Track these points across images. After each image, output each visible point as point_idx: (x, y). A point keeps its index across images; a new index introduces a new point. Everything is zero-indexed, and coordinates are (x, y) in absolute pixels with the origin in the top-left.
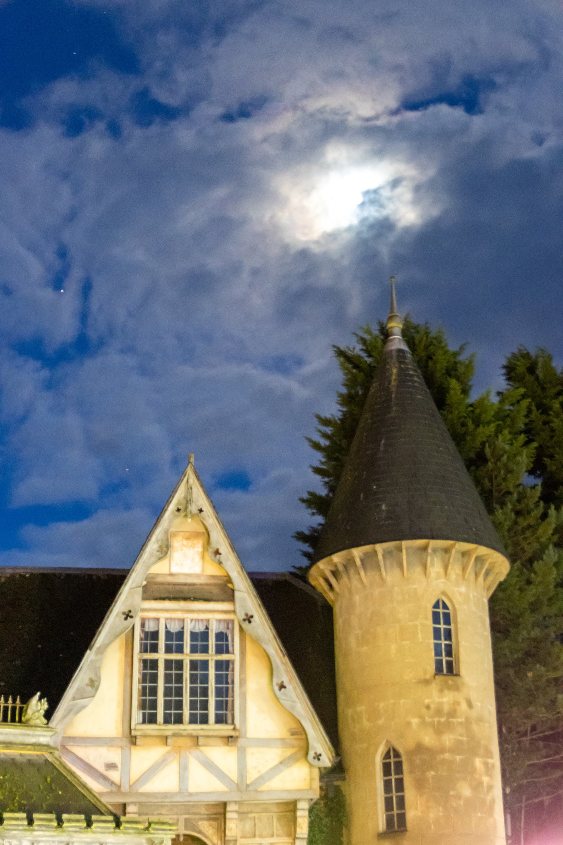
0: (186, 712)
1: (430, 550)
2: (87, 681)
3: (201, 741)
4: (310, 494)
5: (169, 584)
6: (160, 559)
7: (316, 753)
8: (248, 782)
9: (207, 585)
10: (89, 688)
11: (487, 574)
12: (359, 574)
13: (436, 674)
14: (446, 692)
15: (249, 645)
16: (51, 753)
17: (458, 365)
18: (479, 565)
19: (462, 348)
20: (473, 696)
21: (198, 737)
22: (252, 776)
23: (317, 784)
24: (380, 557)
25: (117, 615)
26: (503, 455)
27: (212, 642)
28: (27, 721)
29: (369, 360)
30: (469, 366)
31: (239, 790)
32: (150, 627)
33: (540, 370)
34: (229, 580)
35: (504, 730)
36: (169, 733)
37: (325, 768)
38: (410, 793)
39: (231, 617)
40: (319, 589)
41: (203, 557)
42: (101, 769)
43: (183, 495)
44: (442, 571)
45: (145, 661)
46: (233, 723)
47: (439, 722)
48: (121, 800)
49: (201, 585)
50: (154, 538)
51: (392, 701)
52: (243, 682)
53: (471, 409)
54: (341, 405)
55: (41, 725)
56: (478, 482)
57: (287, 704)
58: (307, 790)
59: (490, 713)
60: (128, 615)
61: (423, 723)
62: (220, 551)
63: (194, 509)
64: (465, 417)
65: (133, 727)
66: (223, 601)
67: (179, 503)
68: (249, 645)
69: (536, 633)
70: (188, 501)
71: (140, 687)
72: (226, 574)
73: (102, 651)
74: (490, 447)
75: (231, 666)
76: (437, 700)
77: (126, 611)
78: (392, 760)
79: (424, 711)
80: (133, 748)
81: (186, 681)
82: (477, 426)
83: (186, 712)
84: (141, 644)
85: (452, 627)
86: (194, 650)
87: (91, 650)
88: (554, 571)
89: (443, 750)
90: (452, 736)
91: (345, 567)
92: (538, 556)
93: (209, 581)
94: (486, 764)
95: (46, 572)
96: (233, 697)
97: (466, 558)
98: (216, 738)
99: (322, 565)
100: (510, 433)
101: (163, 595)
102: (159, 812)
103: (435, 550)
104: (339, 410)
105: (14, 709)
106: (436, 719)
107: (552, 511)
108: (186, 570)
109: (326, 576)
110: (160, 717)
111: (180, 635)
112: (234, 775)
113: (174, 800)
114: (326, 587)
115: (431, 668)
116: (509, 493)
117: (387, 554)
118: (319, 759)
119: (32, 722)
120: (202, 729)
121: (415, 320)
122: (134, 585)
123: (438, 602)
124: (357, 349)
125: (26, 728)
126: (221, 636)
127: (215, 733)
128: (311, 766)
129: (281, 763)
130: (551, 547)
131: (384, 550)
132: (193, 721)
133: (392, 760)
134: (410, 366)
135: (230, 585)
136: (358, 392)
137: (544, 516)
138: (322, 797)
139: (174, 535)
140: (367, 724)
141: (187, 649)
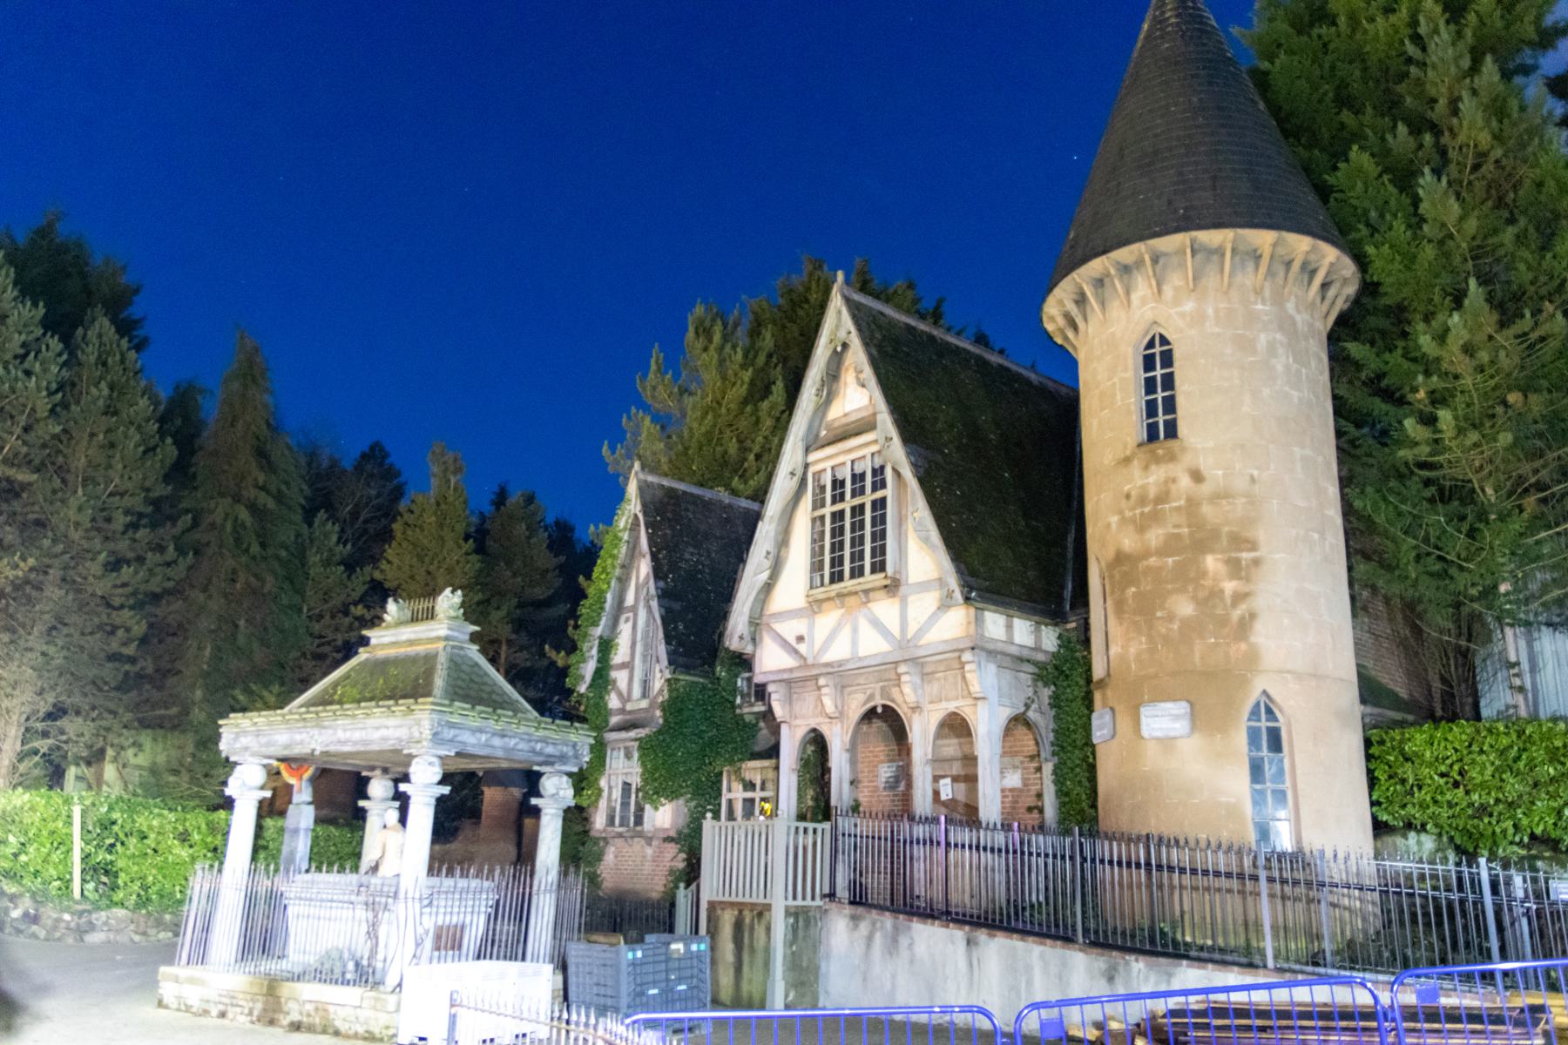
14: (1153, 467)
31: (901, 648)
42: (793, 641)
76: (1140, 483)
90: (1160, 532)
112: (896, 633)
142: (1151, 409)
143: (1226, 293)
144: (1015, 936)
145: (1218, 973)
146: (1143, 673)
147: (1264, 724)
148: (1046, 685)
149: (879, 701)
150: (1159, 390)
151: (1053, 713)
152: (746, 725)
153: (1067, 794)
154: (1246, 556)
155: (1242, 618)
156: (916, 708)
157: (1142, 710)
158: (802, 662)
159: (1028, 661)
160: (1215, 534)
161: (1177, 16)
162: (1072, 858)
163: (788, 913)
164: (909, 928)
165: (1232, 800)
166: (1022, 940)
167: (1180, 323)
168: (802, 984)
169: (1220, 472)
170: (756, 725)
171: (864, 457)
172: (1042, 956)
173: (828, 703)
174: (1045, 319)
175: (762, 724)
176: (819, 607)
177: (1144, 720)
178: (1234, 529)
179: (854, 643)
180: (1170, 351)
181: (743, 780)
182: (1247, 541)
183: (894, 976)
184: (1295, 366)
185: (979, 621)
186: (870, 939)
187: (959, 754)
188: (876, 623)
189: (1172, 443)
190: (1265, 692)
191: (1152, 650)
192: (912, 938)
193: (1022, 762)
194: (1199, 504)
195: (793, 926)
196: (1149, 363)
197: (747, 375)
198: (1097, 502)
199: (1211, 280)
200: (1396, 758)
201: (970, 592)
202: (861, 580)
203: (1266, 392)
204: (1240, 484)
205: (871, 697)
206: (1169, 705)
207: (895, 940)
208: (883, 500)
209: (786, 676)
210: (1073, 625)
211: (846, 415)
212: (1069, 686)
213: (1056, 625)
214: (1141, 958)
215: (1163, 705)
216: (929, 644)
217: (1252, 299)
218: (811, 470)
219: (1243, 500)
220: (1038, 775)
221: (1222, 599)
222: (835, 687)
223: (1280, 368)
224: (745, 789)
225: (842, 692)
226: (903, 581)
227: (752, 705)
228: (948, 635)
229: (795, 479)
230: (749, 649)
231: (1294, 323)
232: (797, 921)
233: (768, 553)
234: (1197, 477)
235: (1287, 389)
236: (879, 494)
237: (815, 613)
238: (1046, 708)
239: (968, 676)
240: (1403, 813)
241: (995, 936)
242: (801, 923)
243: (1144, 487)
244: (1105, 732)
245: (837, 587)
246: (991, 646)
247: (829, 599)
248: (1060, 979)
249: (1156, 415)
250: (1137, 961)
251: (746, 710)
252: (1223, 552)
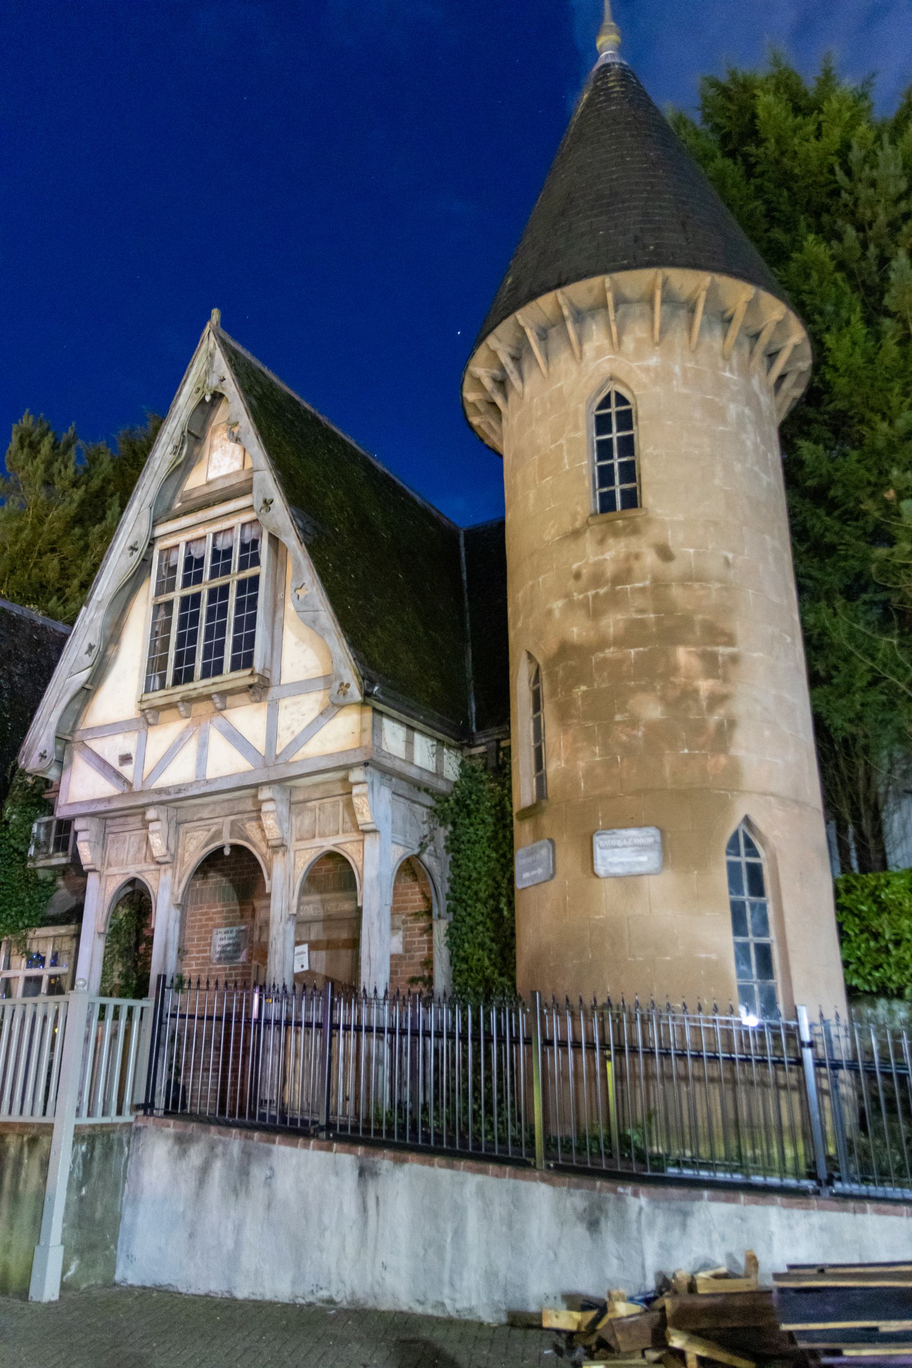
14: (611, 541)
76: (592, 559)
79: (571, 583)
112: (260, 745)
129: (321, 714)
142: (605, 475)
143: (694, 352)
144: (437, 1160)
145: (754, 1207)
146: (597, 792)
147: (744, 859)
148: (443, 822)
149: (227, 840)
150: (616, 455)
151: (449, 858)
152: (38, 883)
153: (465, 960)
154: (723, 650)
155: (720, 725)
156: (279, 847)
157: (596, 839)
158: (126, 789)
159: (426, 790)
160: (687, 622)
161: (621, 86)
162: (464, 1039)
163: (79, 1136)
164: (269, 1153)
165: (714, 957)
166: (451, 1167)
167: (644, 378)
168: (92, 1247)
169: (692, 551)
170: (52, 883)
171: (231, 529)
172: (480, 1191)
173: (158, 844)
174: (467, 382)
175: (60, 882)
176: (156, 717)
177: (598, 852)
178: (708, 617)
179: (201, 760)
180: (629, 412)
181: (28, 954)
182: (723, 633)
183: (239, 1229)
184: (762, 448)
185: (376, 729)
186: (204, 1170)
187: (321, 913)
188: (235, 738)
189: (632, 512)
190: (747, 820)
191: (609, 764)
192: (271, 1169)
193: (404, 922)
194: (667, 586)
195: (84, 1156)
196: (602, 424)
197: (78, 494)
198: (532, 587)
199: (678, 336)
200: (870, 908)
201: (372, 683)
202: (217, 679)
203: (738, 467)
204: (714, 566)
205: (218, 835)
206: (633, 832)
207: (244, 1172)
208: (255, 580)
209: (101, 807)
210: (481, 749)
211: (209, 483)
212: (472, 825)
213: (460, 748)
214: (642, 1190)
215: (624, 833)
216: (305, 760)
217: (721, 363)
218: (159, 546)
219: (718, 585)
220: (425, 937)
221: (696, 700)
222: (169, 823)
223: (749, 444)
224: (29, 966)
225: (177, 831)
226: (274, 681)
227: (49, 857)
229: (136, 554)
230: (52, 774)
231: (759, 403)
232: (91, 1149)
233: (91, 647)
234: (665, 554)
235: (756, 469)
236: (249, 573)
237: (149, 724)
238: (442, 852)
239: (356, 800)
240: (877, 974)
241: (404, 1161)
242: (98, 1152)
243: (600, 564)
244: (540, 871)
245: (183, 689)
246: (388, 763)
247: (171, 706)
248: (510, 1227)
249: (612, 483)
250: (636, 1194)
251: (40, 864)
252: (696, 644)
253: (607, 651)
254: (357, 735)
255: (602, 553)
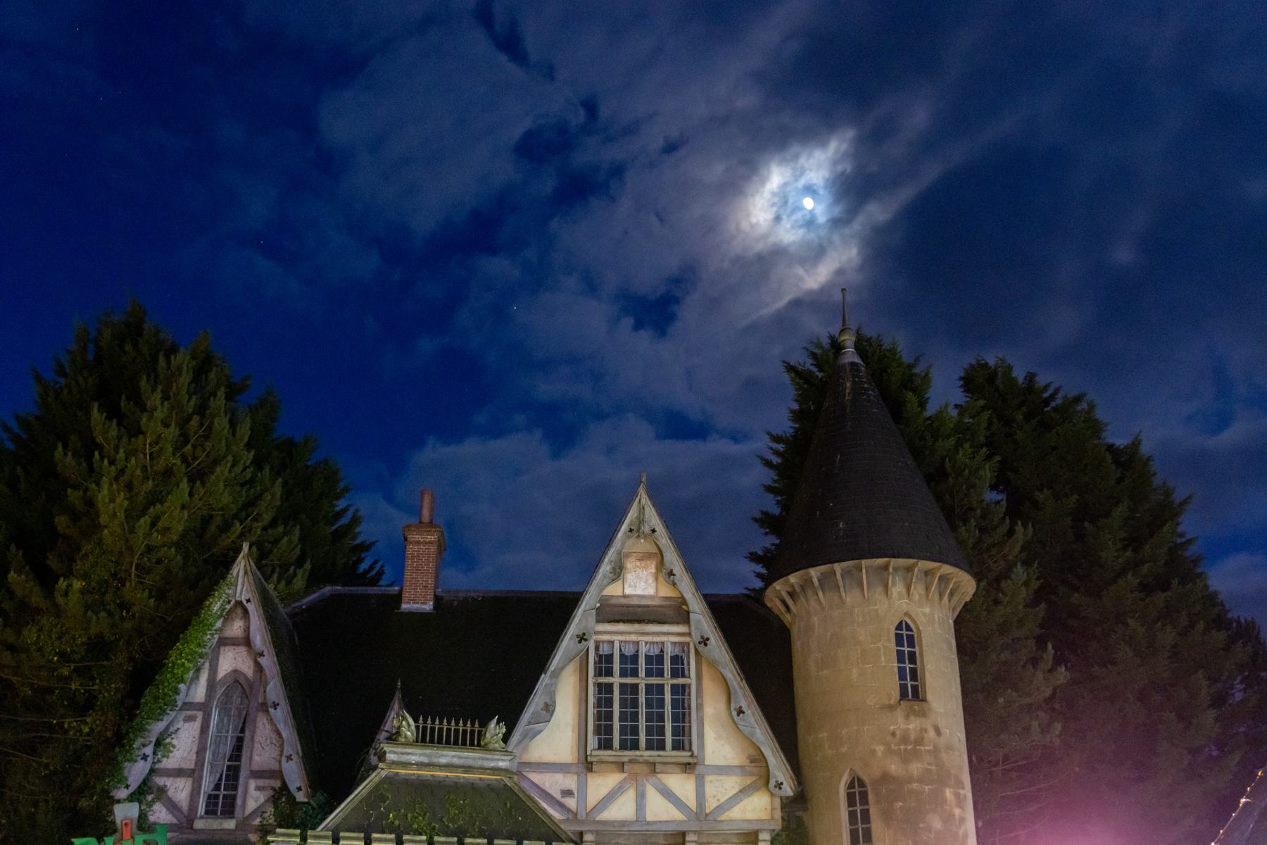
0: (643, 738)
1: (891, 570)
2: (542, 705)
3: (658, 768)
4: (763, 513)
5: (622, 606)
6: (613, 580)
7: (777, 782)
8: (708, 811)
9: (660, 606)
10: (545, 712)
11: (952, 594)
12: (817, 595)
13: (900, 700)
14: (912, 718)
15: (705, 669)
16: (510, 778)
17: (914, 378)
18: (943, 585)
19: (917, 360)
20: (942, 723)
21: (655, 764)
22: (711, 805)
23: (778, 814)
24: (839, 577)
25: (571, 638)
26: (964, 470)
27: (667, 666)
28: (486, 744)
29: (820, 375)
30: (926, 378)
31: (698, 819)
32: (605, 650)
33: (1000, 381)
34: (683, 601)
35: (974, 759)
36: (626, 759)
37: (787, 798)
38: (877, 826)
39: (687, 639)
40: (776, 611)
41: (656, 579)
43: (636, 515)
44: (904, 591)
45: (599, 686)
46: (690, 750)
47: (906, 749)
48: (579, 829)
49: (655, 606)
50: (606, 560)
51: (855, 728)
52: (700, 707)
53: (929, 422)
54: (792, 421)
55: (500, 749)
56: (939, 498)
57: (746, 730)
58: (769, 820)
59: (960, 741)
60: (582, 638)
61: (889, 751)
62: (674, 572)
63: (646, 529)
64: (923, 431)
65: (589, 753)
66: (678, 623)
67: (631, 524)
68: (705, 669)
69: (1005, 655)
70: (641, 520)
71: (595, 712)
72: (680, 596)
73: (556, 674)
74: (950, 462)
75: (687, 691)
76: (903, 726)
77: (581, 634)
78: (857, 790)
79: (889, 738)
80: (589, 775)
81: (642, 705)
82: (936, 440)
83: (643, 738)
84: (595, 668)
85: (917, 649)
86: (649, 673)
87: (545, 674)
88: (1024, 590)
89: (911, 780)
90: (919, 765)
91: (803, 588)
92: (1006, 574)
93: (664, 603)
94: (957, 795)
95: (498, 595)
96: (690, 722)
97: (929, 577)
98: (672, 766)
99: (778, 586)
100: (971, 447)
101: (617, 618)
102: (616, 841)
103: (896, 569)
104: (791, 427)
105: (472, 732)
106: (902, 747)
107: (1019, 528)
108: (639, 592)
109: (782, 596)
110: (616, 744)
111: (635, 658)
112: (692, 803)
113: (631, 829)
114: (783, 609)
115: (896, 693)
116: (971, 509)
117: (846, 573)
118: (780, 788)
119: (491, 746)
120: (659, 756)
121: (870, 332)
122: (587, 608)
123: (901, 622)
124: (808, 364)
125: (485, 752)
126: (676, 660)
127: (673, 760)
128: (772, 795)
129: (740, 791)
130: (1019, 564)
131: (842, 570)
132: (649, 747)
133: (857, 790)
134: (864, 380)
135: (684, 607)
136: (810, 407)
137: (1011, 533)
138: (783, 829)
139: (628, 555)
140: (830, 753)
141: (642, 673)
228: (750, 816)
253: (914, 785)
254: (769, 811)
255: (908, 725)
